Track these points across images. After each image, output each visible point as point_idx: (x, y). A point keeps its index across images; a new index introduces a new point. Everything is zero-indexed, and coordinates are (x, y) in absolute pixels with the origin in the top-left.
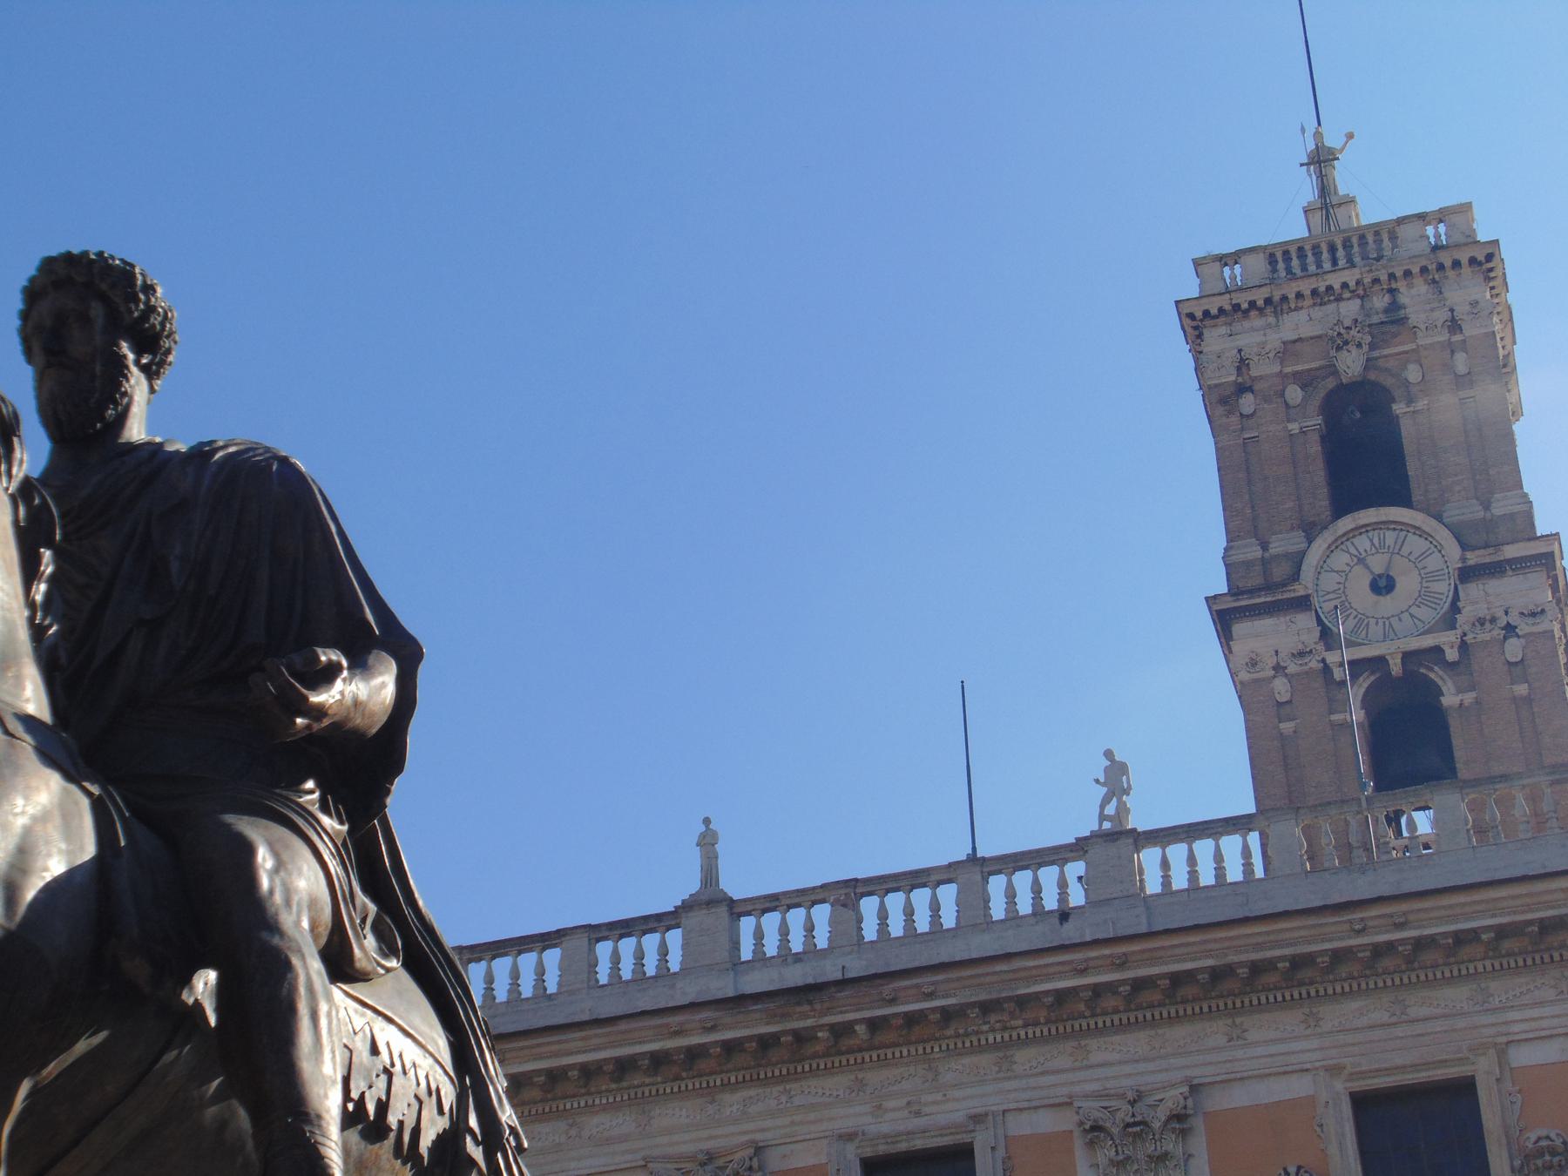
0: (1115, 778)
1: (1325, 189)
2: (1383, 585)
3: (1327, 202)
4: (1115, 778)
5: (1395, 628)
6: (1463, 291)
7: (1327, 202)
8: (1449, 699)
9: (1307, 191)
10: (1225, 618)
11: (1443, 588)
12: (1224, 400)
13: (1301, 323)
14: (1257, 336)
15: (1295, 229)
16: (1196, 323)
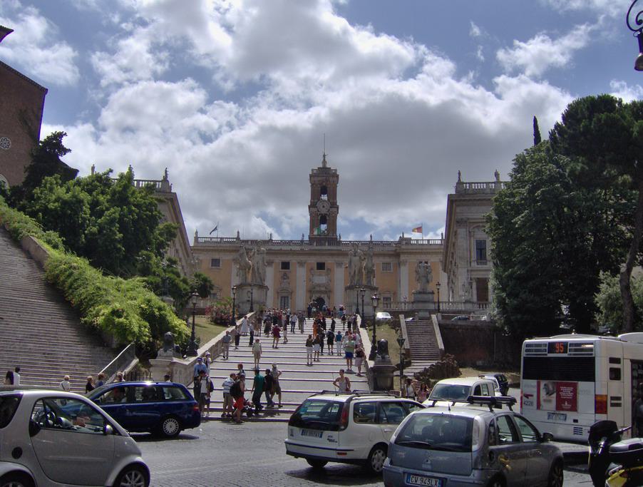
0: (303, 236)
1: (324, 160)
2: (324, 207)
3: (324, 162)
4: (303, 236)
5: (324, 211)
6: (335, 179)
7: (324, 162)
8: (327, 218)
9: (322, 159)
10: (309, 207)
11: (329, 208)
12: (312, 185)
13: (319, 179)
14: (317, 179)
15: (321, 166)
16: (311, 176)
